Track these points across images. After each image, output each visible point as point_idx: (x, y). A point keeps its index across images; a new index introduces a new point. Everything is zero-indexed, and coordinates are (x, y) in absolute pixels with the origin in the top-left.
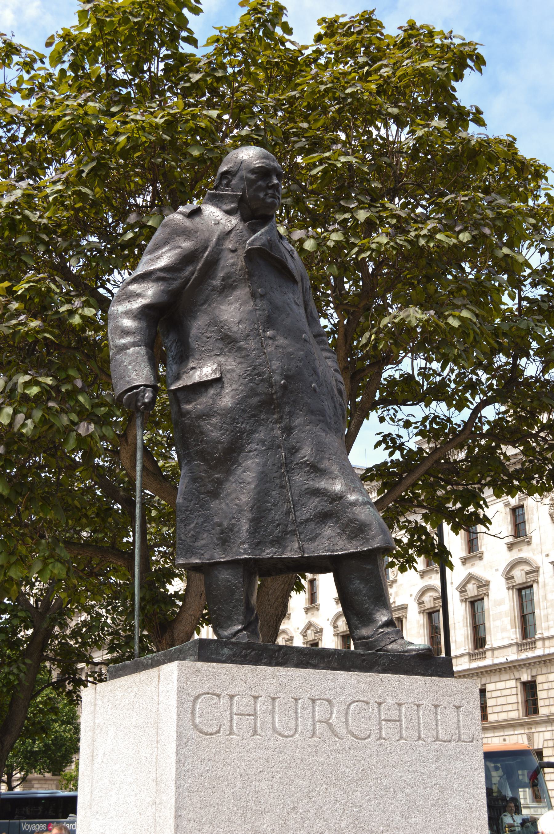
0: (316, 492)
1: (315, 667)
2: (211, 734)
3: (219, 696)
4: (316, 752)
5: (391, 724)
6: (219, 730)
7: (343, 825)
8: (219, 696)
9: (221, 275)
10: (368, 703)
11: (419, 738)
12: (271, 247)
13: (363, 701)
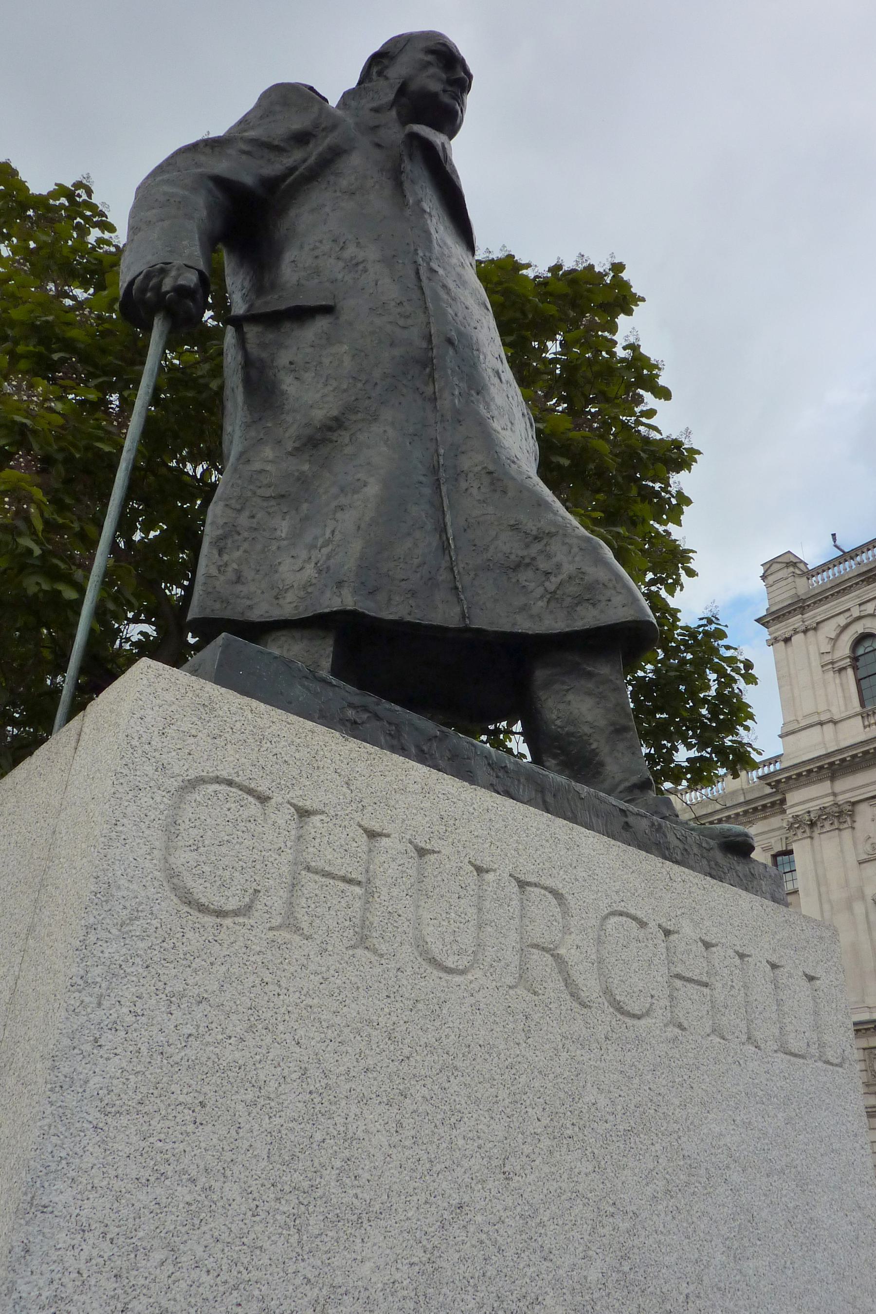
2: (220, 913)
3: (263, 799)
4: (527, 1033)
6: (249, 907)
7: (593, 1275)
8: (263, 799)
10: (642, 924)
13: (634, 918)
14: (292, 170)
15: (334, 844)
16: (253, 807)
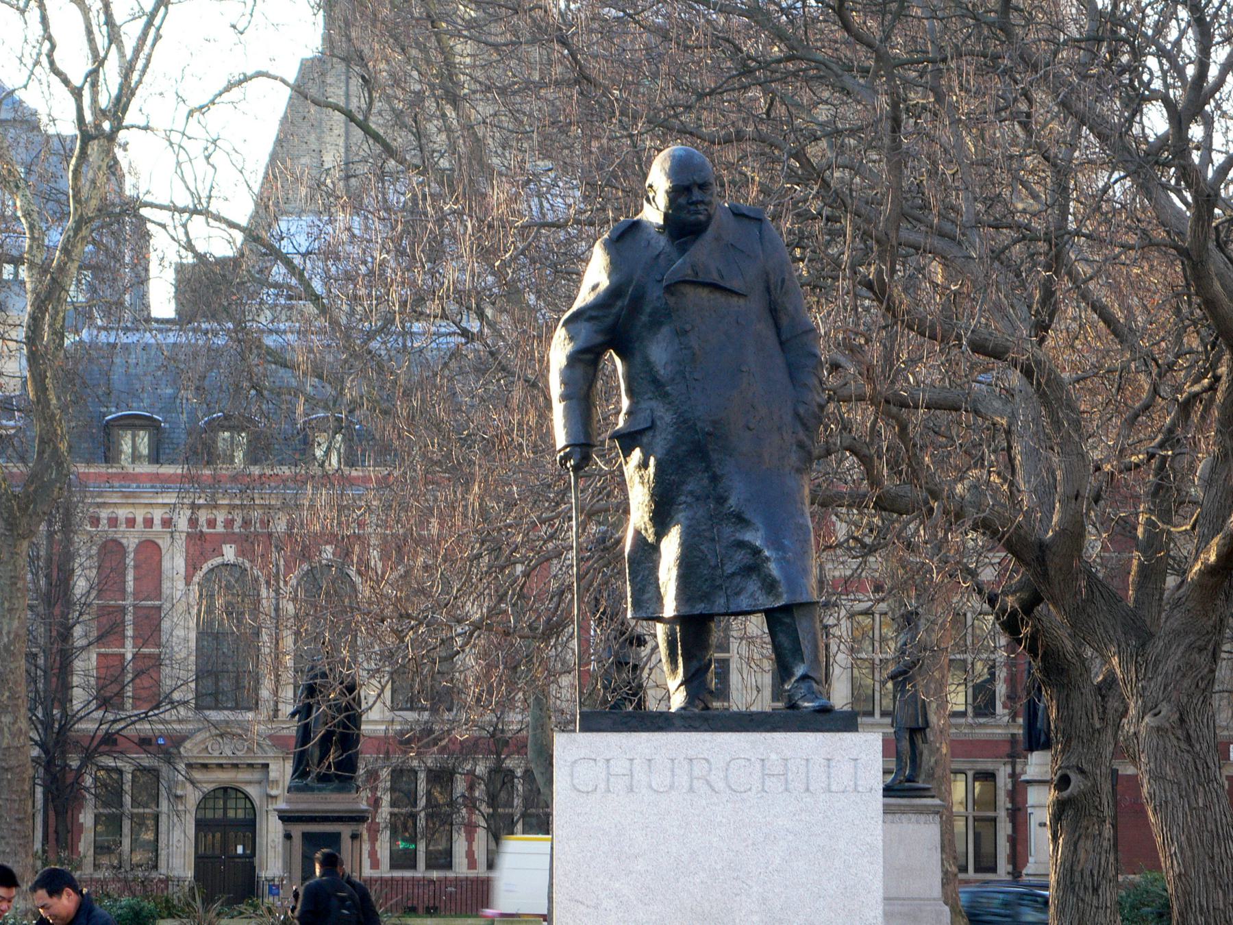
0: (741, 544)
1: (696, 729)
5: (774, 779)
9: (648, 310)
11: (807, 790)
14: (618, 316)
15: (619, 766)
16: (592, 763)
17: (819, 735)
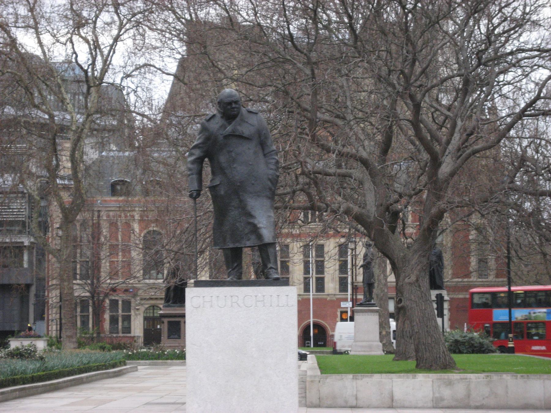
12: (234, 132)
17: (275, 287)
